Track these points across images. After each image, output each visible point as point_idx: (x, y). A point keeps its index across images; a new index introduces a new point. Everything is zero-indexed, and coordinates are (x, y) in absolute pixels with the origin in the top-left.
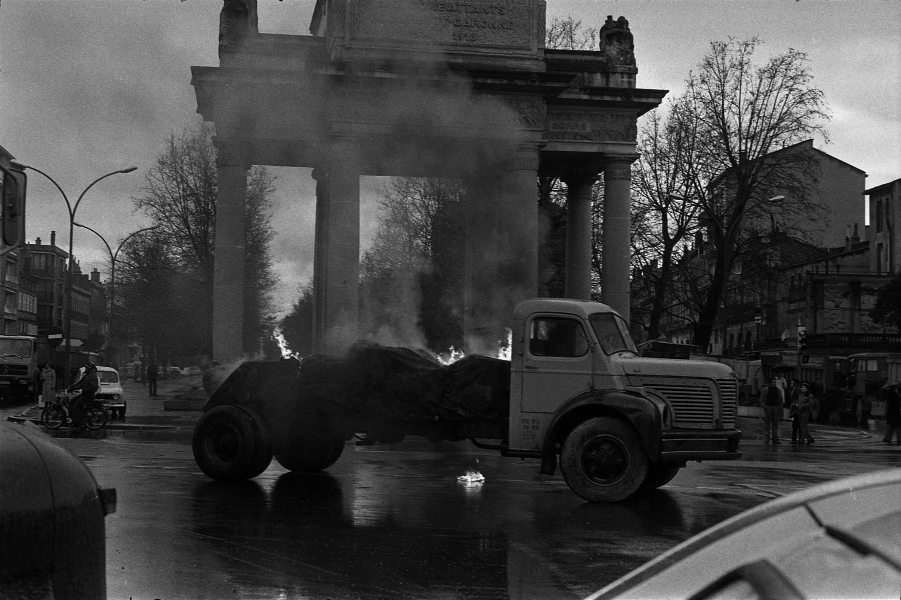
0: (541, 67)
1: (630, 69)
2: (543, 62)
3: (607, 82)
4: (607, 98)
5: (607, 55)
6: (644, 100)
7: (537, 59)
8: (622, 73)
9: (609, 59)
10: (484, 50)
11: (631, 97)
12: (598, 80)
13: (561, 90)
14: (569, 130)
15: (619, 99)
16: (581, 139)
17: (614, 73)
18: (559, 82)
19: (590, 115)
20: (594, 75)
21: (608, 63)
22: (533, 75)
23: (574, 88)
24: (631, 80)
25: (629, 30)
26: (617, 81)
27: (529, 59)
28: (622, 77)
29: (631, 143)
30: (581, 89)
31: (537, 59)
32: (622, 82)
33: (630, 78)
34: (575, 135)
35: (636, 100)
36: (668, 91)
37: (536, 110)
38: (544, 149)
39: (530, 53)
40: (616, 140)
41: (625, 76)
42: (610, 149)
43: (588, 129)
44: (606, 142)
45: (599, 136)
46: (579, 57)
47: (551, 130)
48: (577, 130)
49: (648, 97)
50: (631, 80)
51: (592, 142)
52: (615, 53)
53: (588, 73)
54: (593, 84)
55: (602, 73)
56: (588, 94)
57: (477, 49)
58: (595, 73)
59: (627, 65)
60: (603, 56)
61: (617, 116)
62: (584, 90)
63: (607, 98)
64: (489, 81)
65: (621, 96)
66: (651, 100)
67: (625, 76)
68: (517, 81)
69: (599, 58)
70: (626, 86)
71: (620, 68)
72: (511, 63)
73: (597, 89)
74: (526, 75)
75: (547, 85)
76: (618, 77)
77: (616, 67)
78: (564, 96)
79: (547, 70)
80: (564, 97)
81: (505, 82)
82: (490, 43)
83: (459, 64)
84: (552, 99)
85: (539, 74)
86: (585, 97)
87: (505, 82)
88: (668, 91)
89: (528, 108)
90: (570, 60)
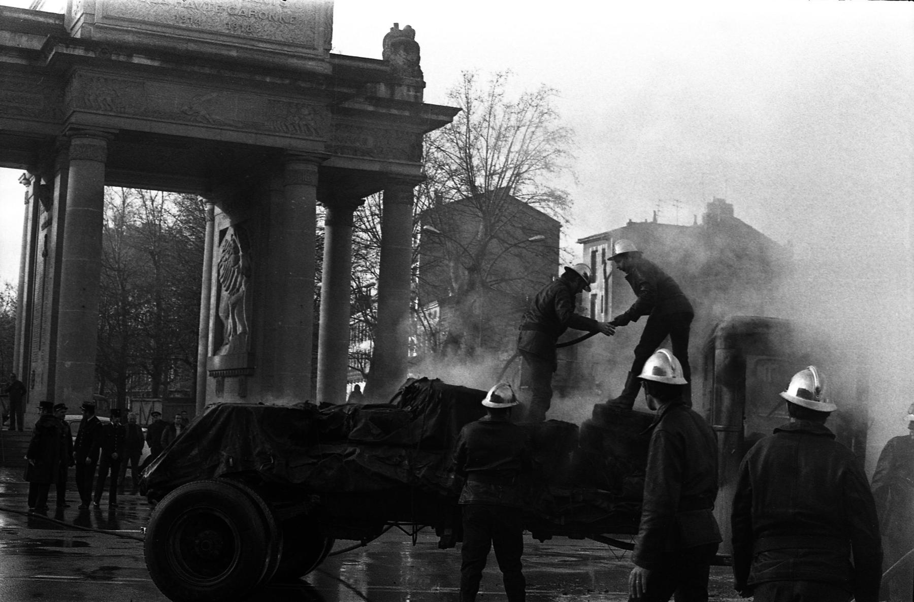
1: (417, 82)
3: (392, 94)
8: (409, 86)
10: (261, 45)
17: (401, 85)
24: (418, 94)
26: (403, 93)
28: (409, 91)
32: (408, 95)
41: (411, 89)
42: (395, 169)
52: (401, 63)
56: (374, 106)
57: (253, 43)
58: (379, 82)
67: (411, 89)
70: (412, 100)
71: (408, 80)
76: (405, 89)
80: (347, 106)
81: (287, 82)
82: (268, 38)
83: (233, 57)
86: (371, 108)
89: (310, 114)
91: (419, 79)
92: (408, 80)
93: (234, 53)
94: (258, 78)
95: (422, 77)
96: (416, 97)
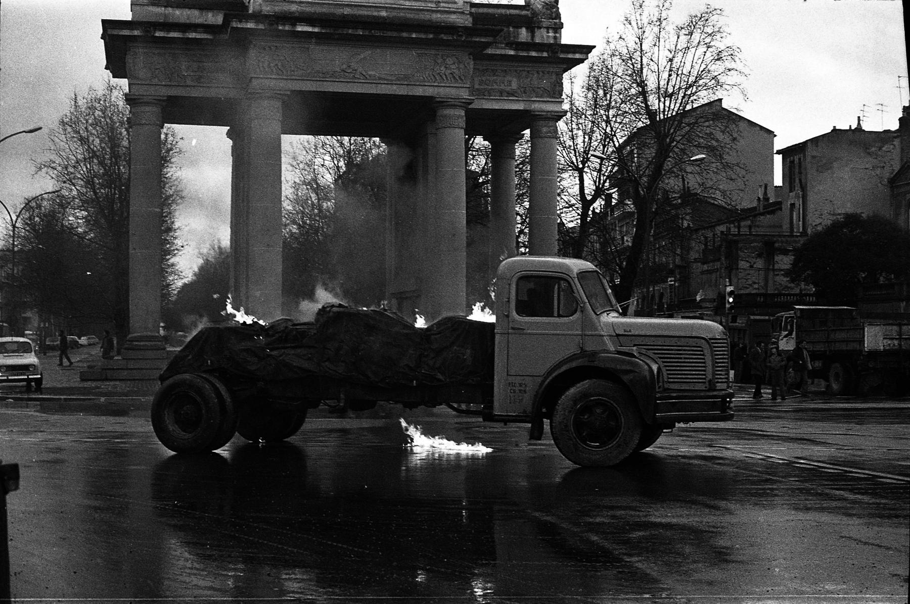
0: (468, 21)
1: (555, 23)
2: (469, 16)
3: (533, 37)
4: (534, 54)
5: (532, 9)
6: (570, 56)
7: (463, 13)
8: (548, 28)
9: (535, 14)
11: (557, 53)
12: (523, 35)
13: (487, 45)
14: (495, 87)
15: (545, 54)
16: (507, 96)
17: (540, 28)
18: (486, 36)
19: (516, 71)
20: (520, 30)
21: (533, 18)
22: (460, 30)
23: (501, 43)
24: (558, 35)
26: (543, 36)
27: (454, 13)
29: (557, 100)
30: (507, 44)
31: (463, 13)
32: (548, 37)
33: (556, 32)
34: (501, 93)
35: (562, 56)
36: (594, 47)
37: (462, 66)
38: (470, 107)
39: (455, 6)
40: (541, 97)
42: (536, 106)
43: (514, 85)
44: (532, 99)
45: (525, 93)
46: (503, 11)
47: (477, 86)
48: (502, 87)
49: (574, 53)
50: (558, 35)
51: (516, 98)
53: (514, 27)
54: (518, 39)
55: (527, 28)
56: (514, 50)
58: (521, 27)
59: (553, 19)
60: (528, 10)
61: (543, 72)
62: (510, 45)
63: (534, 54)
64: (414, 36)
65: (547, 52)
66: (577, 56)
68: (443, 35)
69: (524, 13)
71: (546, 22)
72: (436, 17)
74: (452, 29)
75: (474, 39)
77: (541, 21)
78: (490, 51)
79: (473, 24)
81: (431, 36)
83: (384, 17)
84: (478, 54)
85: (466, 28)
86: (512, 53)
87: (431, 36)
88: (594, 47)
90: (494, 14)
91: (558, 21)
92: (546, 22)
93: (384, 14)
94: (405, 35)
95: (560, 18)
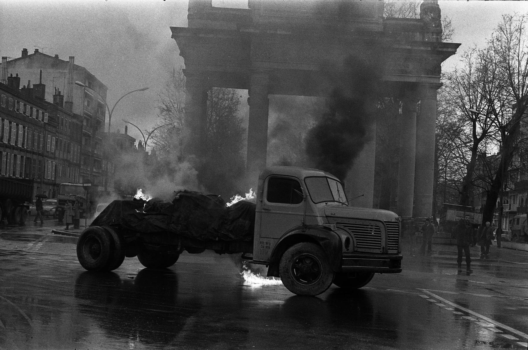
17: (428, 33)
25: (438, 5)
28: (433, 35)
36: (461, 44)
41: (434, 35)
73: (416, 42)
88: (461, 44)
96: (437, 38)
